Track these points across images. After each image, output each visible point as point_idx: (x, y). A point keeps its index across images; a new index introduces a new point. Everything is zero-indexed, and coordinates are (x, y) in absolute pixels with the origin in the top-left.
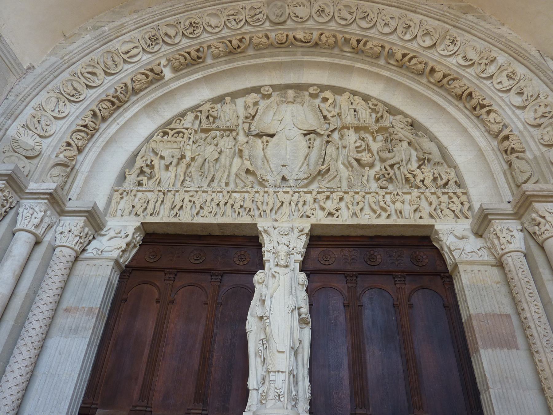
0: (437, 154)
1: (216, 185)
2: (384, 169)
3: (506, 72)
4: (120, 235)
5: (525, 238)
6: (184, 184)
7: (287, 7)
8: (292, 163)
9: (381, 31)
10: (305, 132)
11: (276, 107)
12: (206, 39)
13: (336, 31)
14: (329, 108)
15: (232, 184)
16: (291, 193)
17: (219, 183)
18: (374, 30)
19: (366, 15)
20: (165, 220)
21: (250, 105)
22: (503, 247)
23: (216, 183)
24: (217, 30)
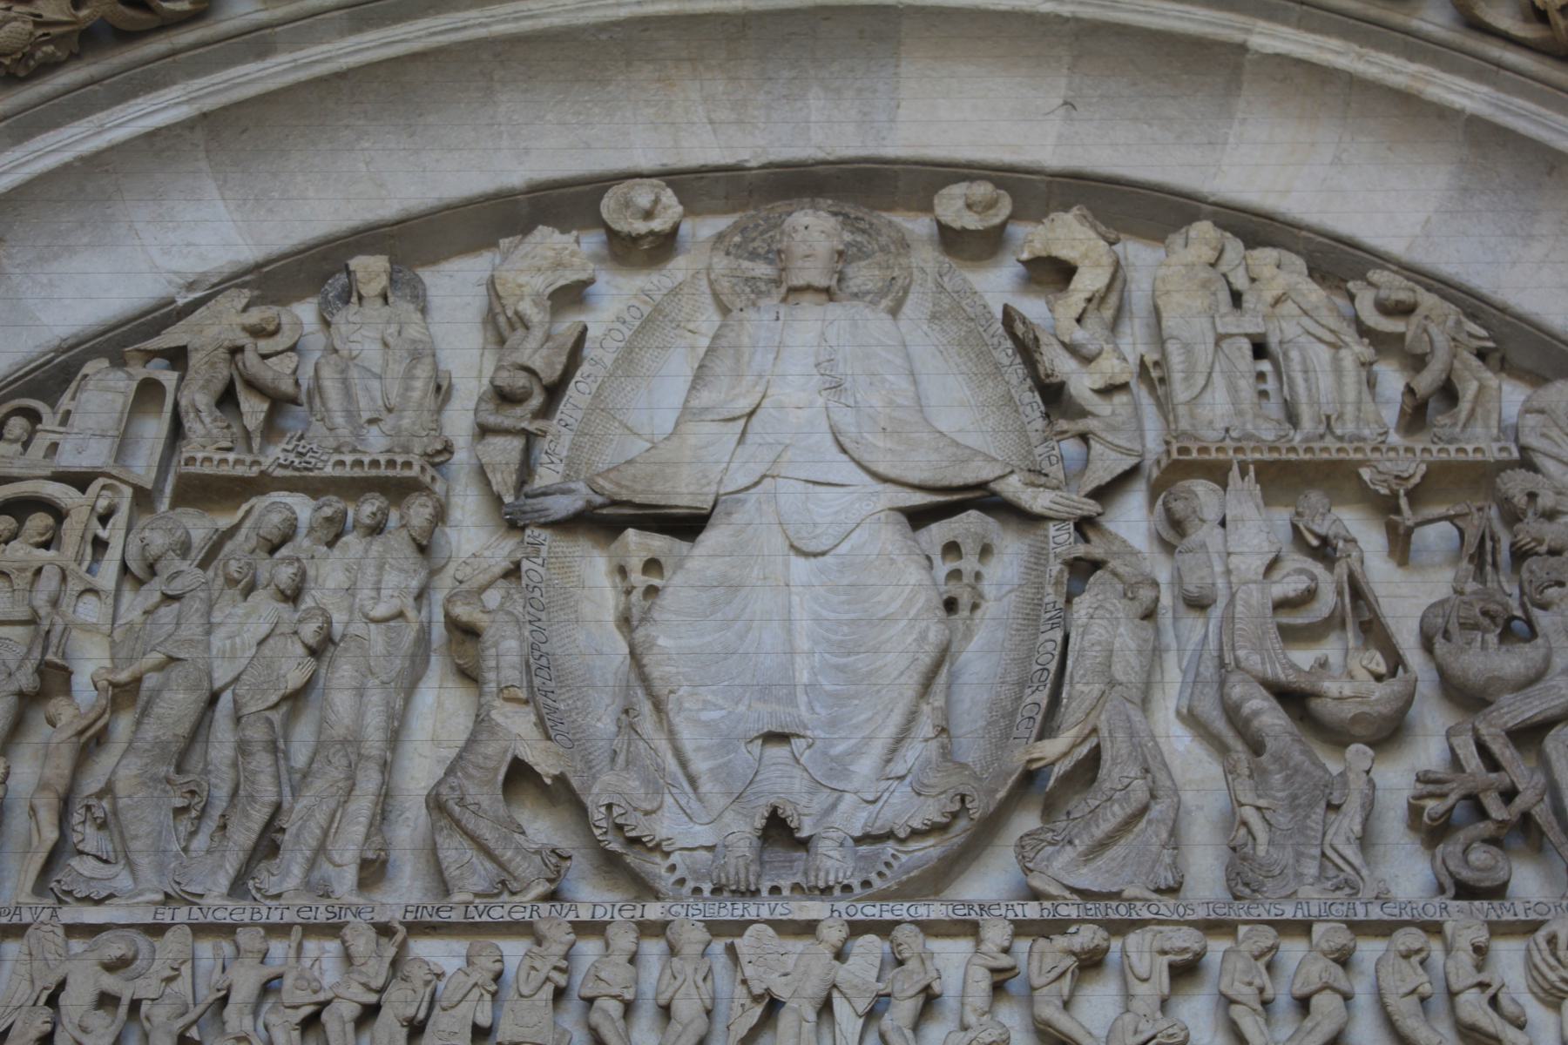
2: (1473, 762)
6: (62, 878)
8: (833, 723)
10: (919, 499)
11: (708, 320)
14: (1079, 335)
15: (408, 870)
16: (833, 933)
17: (312, 864)
21: (527, 307)
23: (297, 871)
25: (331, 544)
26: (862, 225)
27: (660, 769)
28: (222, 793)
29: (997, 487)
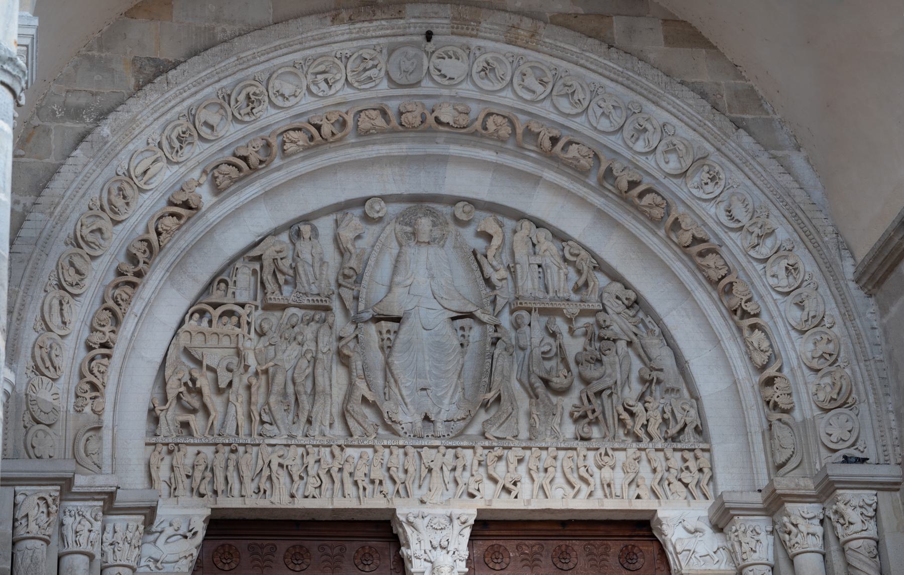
0: (672, 372)
1: (317, 433)
3: (786, 261)
4: (181, 532)
5: (774, 544)
7: (425, 56)
9: (595, 125)
10: (455, 315)
11: (394, 244)
12: (271, 120)
13: (512, 108)
14: (495, 263)
18: (582, 119)
19: (570, 92)
21: (350, 246)
22: (744, 556)
23: (317, 429)
24: (293, 101)
25: (308, 324)
26: (435, 215)
27: (397, 400)
29: (475, 313)
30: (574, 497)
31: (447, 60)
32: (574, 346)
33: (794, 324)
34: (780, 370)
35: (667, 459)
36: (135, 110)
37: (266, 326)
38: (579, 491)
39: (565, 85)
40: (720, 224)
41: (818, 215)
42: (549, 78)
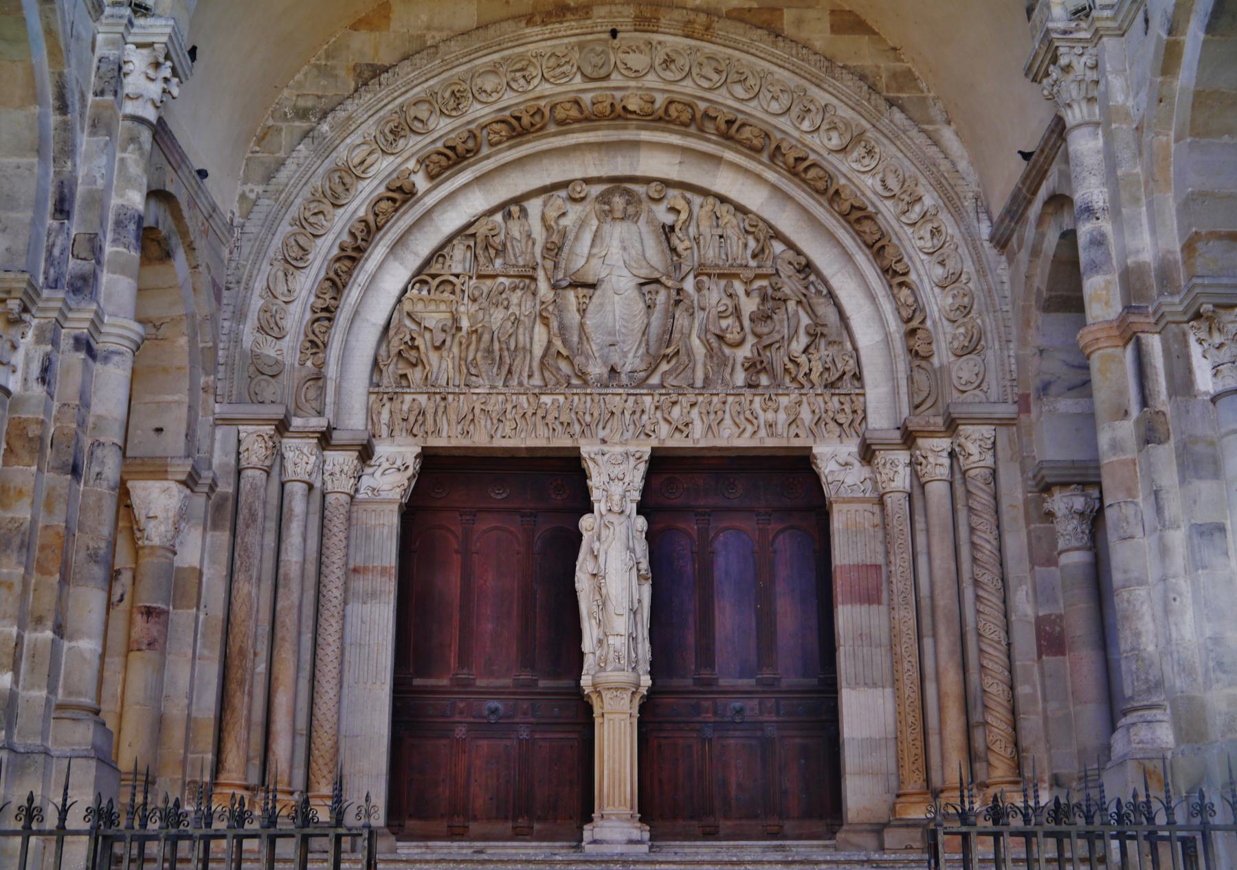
2: (756, 354)
4: (396, 466)
9: (766, 107)
10: (643, 281)
12: (478, 114)
14: (680, 235)
16: (624, 397)
18: (754, 103)
20: (454, 443)
21: (553, 223)
22: (884, 485)
24: (495, 96)
28: (498, 358)
30: (739, 436)
31: (632, 55)
32: (749, 306)
33: (936, 280)
34: (923, 322)
35: (826, 403)
36: (349, 108)
37: (477, 293)
38: (744, 430)
39: (737, 72)
40: (876, 193)
41: (961, 182)
42: (723, 66)
